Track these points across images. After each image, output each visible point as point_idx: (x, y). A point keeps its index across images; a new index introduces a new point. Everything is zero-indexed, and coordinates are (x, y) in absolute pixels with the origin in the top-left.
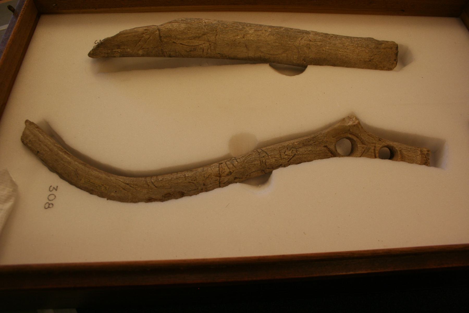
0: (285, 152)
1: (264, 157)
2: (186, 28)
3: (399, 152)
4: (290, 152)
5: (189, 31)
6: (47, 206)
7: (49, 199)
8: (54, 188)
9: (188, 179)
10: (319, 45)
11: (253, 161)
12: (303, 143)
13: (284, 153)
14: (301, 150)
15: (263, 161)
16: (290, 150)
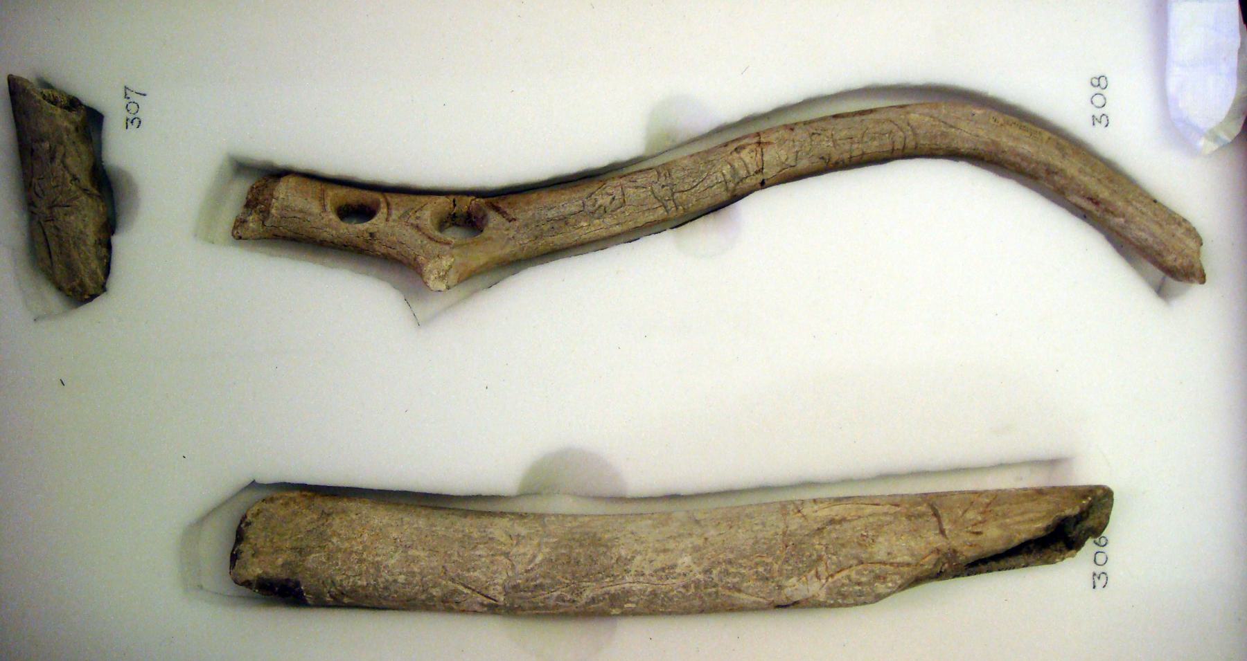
0: (611, 203)
1: (663, 186)
2: (871, 541)
3: (329, 208)
4: (600, 202)
5: (862, 535)
6: (1103, 81)
7: (1101, 97)
8: (1100, 122)
9: (828, 137)
10: (482, 546)
11: (688, 176)
12: (566, 224)
13: (613, 199)
14: (574, 209)
15: (664, 178)
16: (600, 206)
